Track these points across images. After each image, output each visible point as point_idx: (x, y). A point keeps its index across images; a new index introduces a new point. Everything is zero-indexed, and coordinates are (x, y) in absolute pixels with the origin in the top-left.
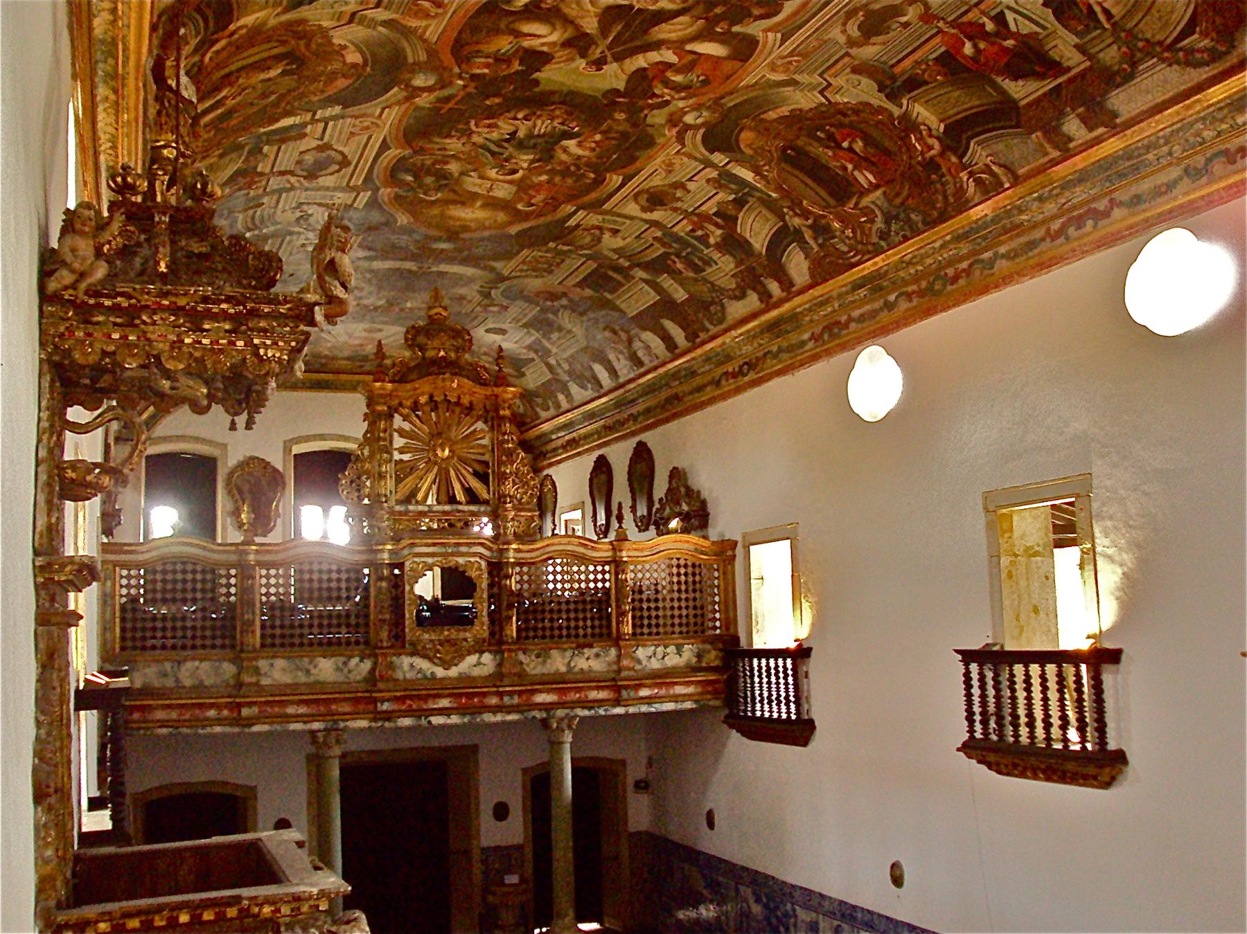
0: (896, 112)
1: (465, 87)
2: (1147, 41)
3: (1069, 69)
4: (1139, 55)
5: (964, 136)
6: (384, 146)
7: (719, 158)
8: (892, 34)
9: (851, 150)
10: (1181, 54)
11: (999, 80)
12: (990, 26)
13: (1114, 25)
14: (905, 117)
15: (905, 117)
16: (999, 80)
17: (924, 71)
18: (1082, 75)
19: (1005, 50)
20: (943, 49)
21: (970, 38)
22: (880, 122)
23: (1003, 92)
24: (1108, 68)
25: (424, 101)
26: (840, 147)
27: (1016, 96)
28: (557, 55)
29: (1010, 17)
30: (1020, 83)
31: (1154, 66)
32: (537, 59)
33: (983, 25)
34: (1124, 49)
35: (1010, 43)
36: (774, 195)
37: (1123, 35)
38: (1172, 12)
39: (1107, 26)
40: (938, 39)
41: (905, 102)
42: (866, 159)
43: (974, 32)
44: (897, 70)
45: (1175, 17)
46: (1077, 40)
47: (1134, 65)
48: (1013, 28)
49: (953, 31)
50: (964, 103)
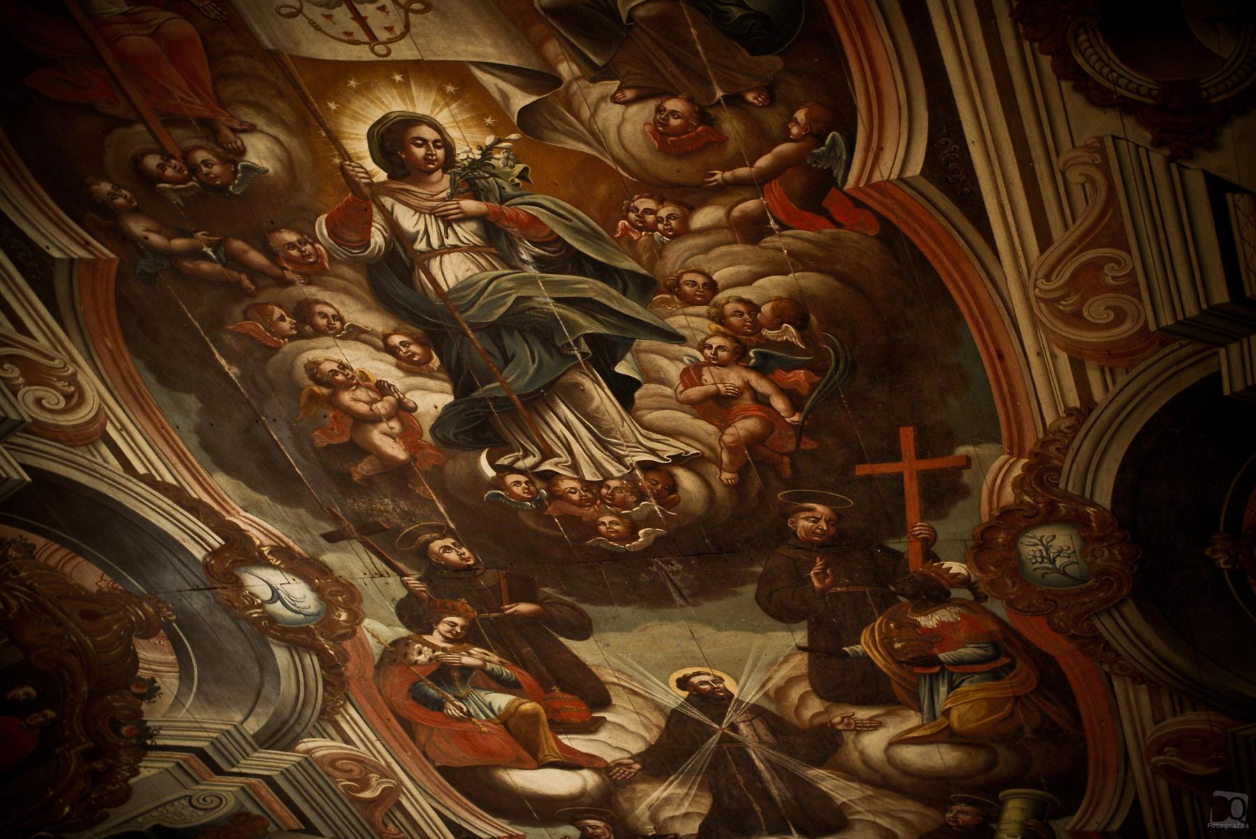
1: (930, 556)
6: (949, 166)
25: (998, 475)
28: (815, 706)
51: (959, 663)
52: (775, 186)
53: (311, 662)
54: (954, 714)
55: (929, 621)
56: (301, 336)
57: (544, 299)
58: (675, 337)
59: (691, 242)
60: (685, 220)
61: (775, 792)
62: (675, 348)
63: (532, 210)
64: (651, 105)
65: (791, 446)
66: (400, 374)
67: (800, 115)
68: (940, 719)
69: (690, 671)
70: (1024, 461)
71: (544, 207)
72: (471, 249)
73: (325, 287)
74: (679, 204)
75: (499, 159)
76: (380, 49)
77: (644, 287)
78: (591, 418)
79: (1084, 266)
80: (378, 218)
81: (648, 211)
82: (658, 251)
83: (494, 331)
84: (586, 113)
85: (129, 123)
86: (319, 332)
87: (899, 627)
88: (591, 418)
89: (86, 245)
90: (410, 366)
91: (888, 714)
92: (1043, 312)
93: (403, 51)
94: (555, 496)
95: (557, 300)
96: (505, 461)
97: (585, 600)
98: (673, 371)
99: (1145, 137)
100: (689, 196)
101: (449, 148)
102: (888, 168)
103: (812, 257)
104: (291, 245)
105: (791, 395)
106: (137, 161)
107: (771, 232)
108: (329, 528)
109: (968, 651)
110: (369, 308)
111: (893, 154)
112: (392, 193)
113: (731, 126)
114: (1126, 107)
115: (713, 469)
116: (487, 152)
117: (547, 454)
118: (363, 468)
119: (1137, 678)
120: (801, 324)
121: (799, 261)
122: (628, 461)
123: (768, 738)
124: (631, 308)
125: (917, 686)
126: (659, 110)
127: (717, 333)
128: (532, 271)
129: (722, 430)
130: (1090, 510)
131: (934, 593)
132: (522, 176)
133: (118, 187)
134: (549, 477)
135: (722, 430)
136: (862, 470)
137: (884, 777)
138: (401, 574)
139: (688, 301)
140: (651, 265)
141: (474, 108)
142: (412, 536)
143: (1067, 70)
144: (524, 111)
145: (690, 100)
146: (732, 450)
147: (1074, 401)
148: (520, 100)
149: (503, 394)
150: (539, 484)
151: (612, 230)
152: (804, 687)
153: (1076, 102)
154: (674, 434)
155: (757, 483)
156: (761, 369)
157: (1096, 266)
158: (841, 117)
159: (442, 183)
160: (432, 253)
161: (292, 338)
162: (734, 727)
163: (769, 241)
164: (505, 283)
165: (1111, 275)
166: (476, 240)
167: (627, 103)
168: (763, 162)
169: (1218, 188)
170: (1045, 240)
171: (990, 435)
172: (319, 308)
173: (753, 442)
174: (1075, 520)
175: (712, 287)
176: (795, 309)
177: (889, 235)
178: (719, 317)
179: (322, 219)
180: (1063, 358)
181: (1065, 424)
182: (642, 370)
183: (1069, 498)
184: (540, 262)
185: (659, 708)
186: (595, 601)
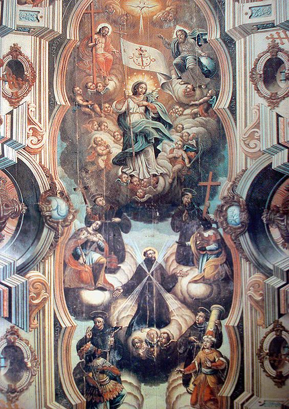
6: (232, 108)
28: (175, 264)
32: (185, 258)
51: (210, 251)
52: (201, 106)
55: (206, 234)
56: (97, 130)
60: (183, 112)
62: (171, 143)
63: (156, 106)
68: (202, 272)
71: (159, 107)
72: (141, 113)
74: (183, 107)
76: (143, 67)
77: (169, 126)
81: (177, 109)
84: (173, 86)
86: (101, 130)
87: (199, 236)
91: (191, 269)
93: (147, 69)
100: (185, 106)
101: (146, 90)
103: (204, 124)
106: (87, 84)
107: (197, 117)
109: (213, 246)
111: (223, 103)
113: (198, 92)
121: (202, 125)
124: (166, 132)
133: (80, 88)
137: (184, 298)
139: (177, 132)
147: (244, 168)
148: (163, 81)
152: (174, 257)
159: (142, 97)
166: (143, 112)
168: (201, 101)
170: (246, 126)
173: (180, 170)
175: (183, 128)
176: (195, 137)
177: (219, 121)
178: (182, 137)
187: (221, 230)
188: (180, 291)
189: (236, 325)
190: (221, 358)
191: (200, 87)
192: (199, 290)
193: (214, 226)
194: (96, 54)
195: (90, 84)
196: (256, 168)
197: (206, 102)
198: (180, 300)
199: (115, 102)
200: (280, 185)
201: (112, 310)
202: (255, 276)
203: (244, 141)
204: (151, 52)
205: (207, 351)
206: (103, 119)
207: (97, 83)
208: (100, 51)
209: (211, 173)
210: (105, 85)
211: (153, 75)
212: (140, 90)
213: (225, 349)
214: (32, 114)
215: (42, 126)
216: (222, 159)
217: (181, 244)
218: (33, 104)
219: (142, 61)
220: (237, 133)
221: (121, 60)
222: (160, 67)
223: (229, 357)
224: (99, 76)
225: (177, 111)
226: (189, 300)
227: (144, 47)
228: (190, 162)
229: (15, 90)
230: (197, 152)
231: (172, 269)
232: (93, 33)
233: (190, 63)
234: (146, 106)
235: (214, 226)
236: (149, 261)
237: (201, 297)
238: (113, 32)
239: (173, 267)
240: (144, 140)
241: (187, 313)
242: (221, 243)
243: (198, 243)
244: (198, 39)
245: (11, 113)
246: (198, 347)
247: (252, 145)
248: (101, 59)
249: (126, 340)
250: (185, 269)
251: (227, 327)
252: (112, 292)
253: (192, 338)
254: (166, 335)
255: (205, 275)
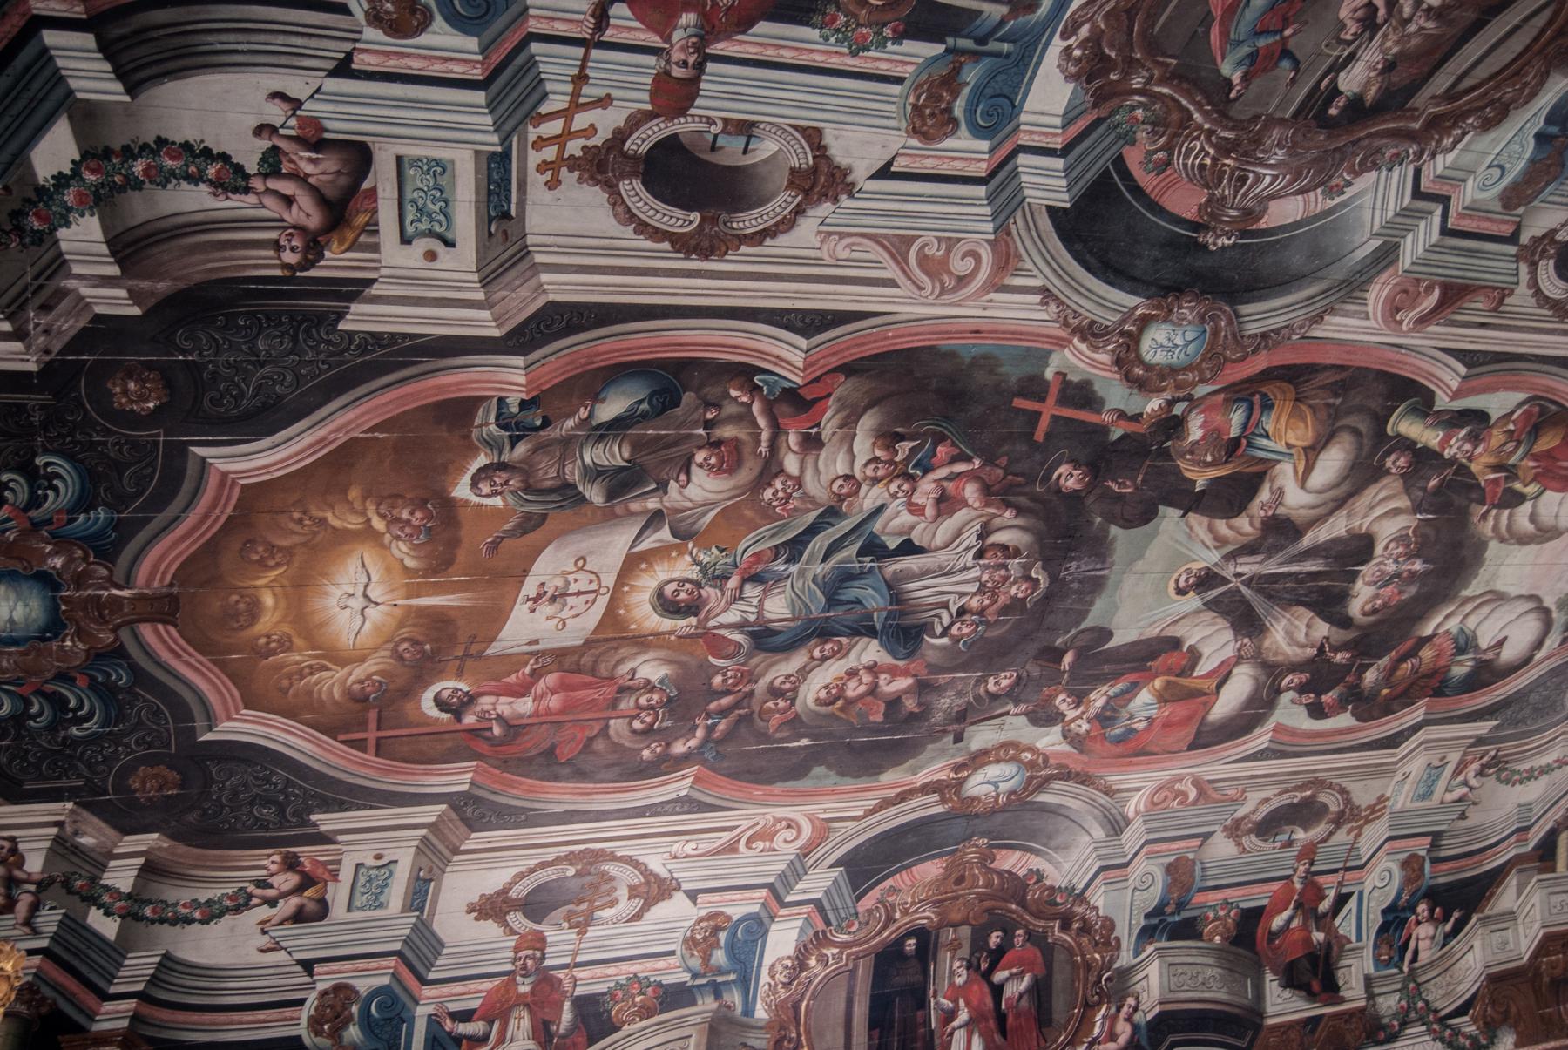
0: (1125, 958)
2: (1427, 1003)
3: (1342, 1001)
4: (1413, 1015)
5: (1171, 1038)
7: (819, 881)
8: (1268, 845)
9: (997, 990)
10: (1448, 1032)
11: (1269, 976)
12: (1324, 906)
13: (1412, 970)
14: (1125, 973)
15: (1125, 973)
16: (1269, 976)
17: (1216, 918)
18: (1351, 1014)
19: (1308, 940)
20: (1265, 902)
21: (1299, 906)
22: (1088, 966)
23: (1259, 995)
24: (1378, 1018)
26: (987, 975)
27: (1270, 1009)
28: (1243, 523)
29: (1352, 904)
30: (1287, 993)
31: (1419, 1035)
33: (1323, 898)
34: (1404, 1003)
35: (1318, 937)
36: (761, 1013)
37: (1412, 985)
38: (1460, 983)
39: (1406, 969)
40: (1275, 886)
41: (1150, 949)
42: (1001, 1018)
43: (1307, 902)
44: (1199, 898)
45: (1462, 988)
46: (1371, 970)
47: (1404, 1024)
48: (1337, 922)
49: (1298, 886)
50: (1209, 989)
51: (1245, 426)
53: (1058, 785)
54: (1292, 441)
56: (793, 700)
57: (819, 569)
58: (880, 510)
59: (808, 477)
60: (790, 477)
61: (1314, 569)
62: (888, 512)
64: (694, 468)
65: (1000, 472)
66: (843, 661)
67: (734, 393)
69: (1172, 585)
70: (1075, 341)
71: (749, 545)
73: (762, 675)
74: (776, 476)
75: (704, 558)
76: (603, 591)
77: (832, 513)
78: (925, 573)
79: (920, 265)
80: (722, 632)
81: (775, 493)
82: (806, 497)
83: (832, 601)
84: (689, 504)
85: (607, 726)
86: (795, 690)
87: (1192, 453)
88: (925, 573)
89: (683, 777)
90: (841, 653)
91: (1272, 480)
92: (947, 298)
93: (609, 580)
94: (981, 612)
95: (823, 561)
96: (938, 630)
97: (1078, 623)
98: (906, 518)
99: (826, 208)
100: (771, 469)
102: (798, 359)
103: (848, 416)
104: (725, 681)
105: (953, 460)
106: (634, 732)
107: (819, 434)
108: (951, 738)
110: (787, 659)
112: (707, 619)
113: (727, 432)
114: (799, 211)
115: (997, 522)
116: (696, 562)
117: (945, 605)
118: (910, 704)
119: (1318, 319)
120: (902, 437)
122: (970, 564)
123: (1259, 558)
124: (845, 526)
125: (1254, 458)
126: (701, 466)
127: (887, 485)
128: (794, 568)
129: (967, 505)
130: (1139, 312)
131: (1172, 425)
132: (722, 551)
133: (648, 747)
134: (962, 611)
135: (967, 505)
136: (1039, 436)
138: (1007, 713)
140: (817, 505)
141: (662, 559)
142: (978, 698)
143: (759, 237)
144: (674, 533)
145: (700, 448)
146: (988, 505)
147: (1037, 298)
148: (665, 534)
149: (884, 614)
150: (967, 617)
151: (781, 517)
152: (1221, 526)
153: (782, 239)
154: (959, 533)
155: (1022, 500)
156: (926, 471)
157: (923, 260)
158: (745, 374)
159: (709, 592)
160: (760, 613)
161: (793, 704)
162: (1238, 575)
163: (825, 436)
164: (799, 585)
165: (934, 251)
166: (760, 588)
167: (689, 481)
168: (762, 422)
169: (885, 173)
170: (891, 283)
171: (1045, 357)
172: (777, 683)
173: (987, 491)
174: (1145, 322)
175: (848, 477)
176: (888, 438)
177: (849, 370)
178: (875, 481)
179: (712, 660)
180: (992, 296)
181: (1053, 307)
182: (900, 534)
183: (1123, 322)
184: (791, 560)
185: (1197, 612)
186: (1083, 615)
187: (1201, 391)
188: (1312, 512)
189: (1463, 370)
190: (1515, 416)
191: (708, 425)
192: (1332, 463)
193: (1178, 409)
194: (536, 714)
195: (637, 725)
196: (1050, 259)
197: (769, 411)
198: (1332, 512)
199: (712, 660)
200: (1137, 190)
201: (1280, 658)
202: (1371, 303)
203: (943, 291)
204: (549, 567)
205: (1479, 450)
206: (763, 683)
207: (638, 706)
208: (525, 705)
209: (1018, 402)
210: (648, 686)
211: (633, 563)
212: (683, 596)
213: (1499, 403)
214: (704, 847)
215: (745, 824)
216: (986, 362)
217: (1191, 501)
218: (675, 848)
219: (578, 594)
220: (911, 308)
221: (559, 655)
222: (615, 544)
223: (1522, 396)
224: (614, 704)
225: (780, 495)
226: (1344, 488)
227: (530, 588)
228: (969, 460)
229: (623, 893)
230: (940, 439)
231: (1247, 528)
232: (458, 727)
233: (614, 455)
234: (744, 581)
235: (1178, 409)
236: (1206, 580)
237: (1351, 457)
238: (459, 674)
239: (1246, 525)
240: (856, 583)
241: (1371, 493)
242: (1240, 393)
243: (1209, 459)
244: (516, 429)
245: (693, 895)
246: (1463, 470)
247: (961, 266)
248: (554, 702)
249: (1360, 627)
250: (1265, 495)
251: (1456, 395)
252: (1239, 659)
253: (1433, 483)
254: (1392, 545)
255: (1305, 444)
